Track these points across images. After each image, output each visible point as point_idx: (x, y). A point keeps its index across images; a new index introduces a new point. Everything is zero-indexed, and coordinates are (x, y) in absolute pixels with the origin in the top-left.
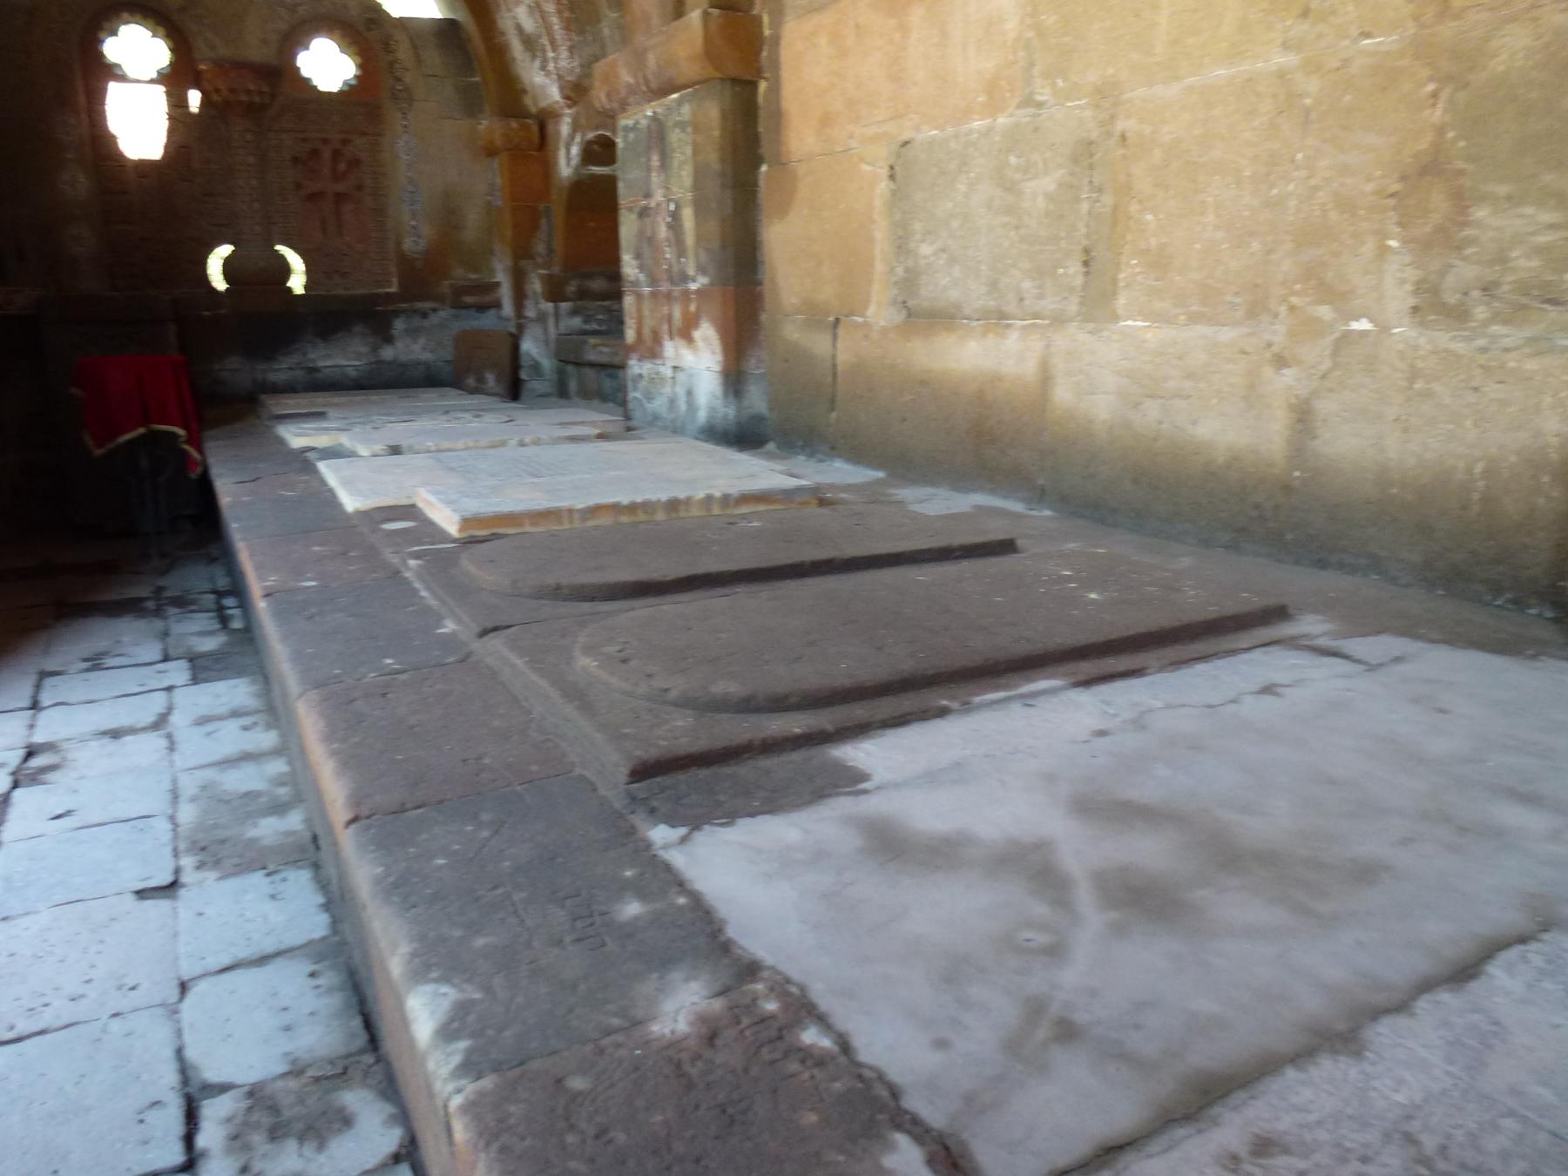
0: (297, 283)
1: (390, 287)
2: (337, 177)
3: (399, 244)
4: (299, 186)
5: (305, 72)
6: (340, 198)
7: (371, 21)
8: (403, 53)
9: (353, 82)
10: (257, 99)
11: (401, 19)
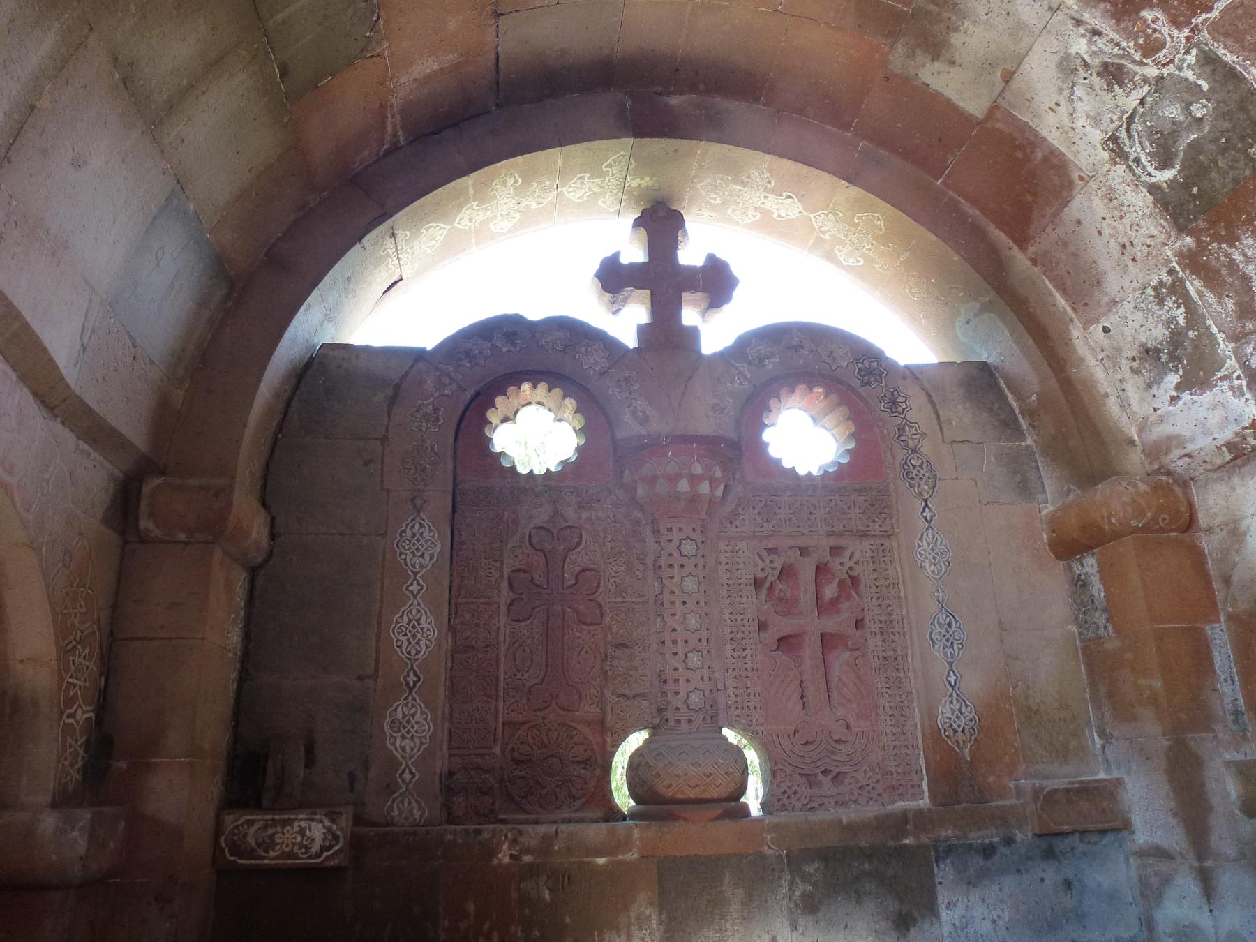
0: (753, 798)
1: (914, 797)
2: (824, 608)
3: (931, 714)
4: (762, 626)
5: (774, 452)
6: (828, 641)
7: (869, 372)
8: (917, 411)
9: (845, 460)
10: (704, 488)
11: (907, 367)
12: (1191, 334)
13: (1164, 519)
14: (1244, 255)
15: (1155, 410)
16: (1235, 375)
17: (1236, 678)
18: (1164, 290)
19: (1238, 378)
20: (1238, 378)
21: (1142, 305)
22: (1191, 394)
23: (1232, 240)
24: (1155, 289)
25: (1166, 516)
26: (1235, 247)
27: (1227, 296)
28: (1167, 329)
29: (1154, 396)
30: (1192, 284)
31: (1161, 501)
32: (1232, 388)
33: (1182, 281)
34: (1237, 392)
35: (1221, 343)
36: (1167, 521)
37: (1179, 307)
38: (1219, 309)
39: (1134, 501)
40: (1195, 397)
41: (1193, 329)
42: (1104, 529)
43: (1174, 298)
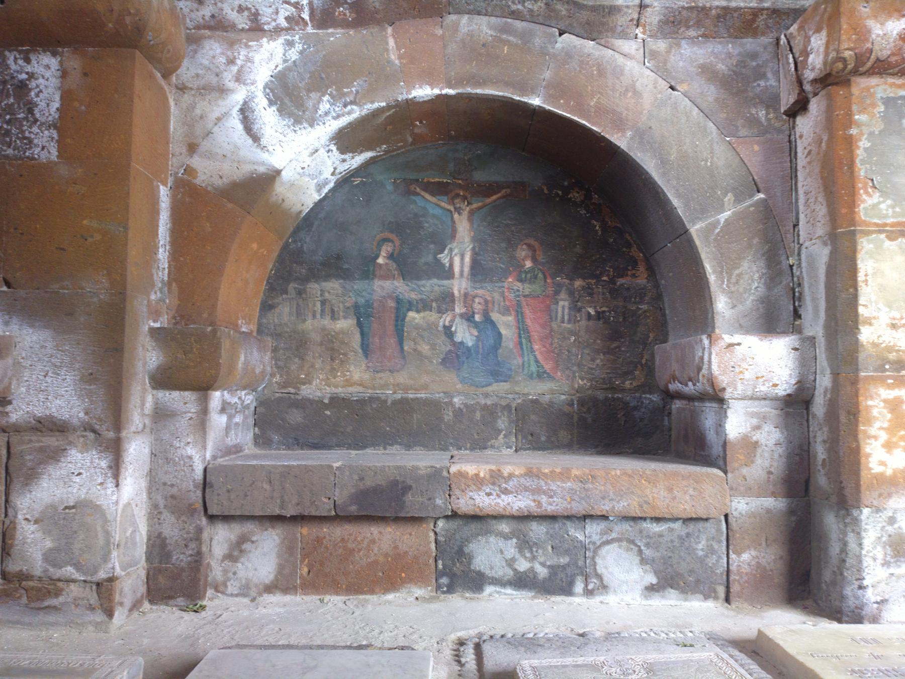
36: (168, 56)
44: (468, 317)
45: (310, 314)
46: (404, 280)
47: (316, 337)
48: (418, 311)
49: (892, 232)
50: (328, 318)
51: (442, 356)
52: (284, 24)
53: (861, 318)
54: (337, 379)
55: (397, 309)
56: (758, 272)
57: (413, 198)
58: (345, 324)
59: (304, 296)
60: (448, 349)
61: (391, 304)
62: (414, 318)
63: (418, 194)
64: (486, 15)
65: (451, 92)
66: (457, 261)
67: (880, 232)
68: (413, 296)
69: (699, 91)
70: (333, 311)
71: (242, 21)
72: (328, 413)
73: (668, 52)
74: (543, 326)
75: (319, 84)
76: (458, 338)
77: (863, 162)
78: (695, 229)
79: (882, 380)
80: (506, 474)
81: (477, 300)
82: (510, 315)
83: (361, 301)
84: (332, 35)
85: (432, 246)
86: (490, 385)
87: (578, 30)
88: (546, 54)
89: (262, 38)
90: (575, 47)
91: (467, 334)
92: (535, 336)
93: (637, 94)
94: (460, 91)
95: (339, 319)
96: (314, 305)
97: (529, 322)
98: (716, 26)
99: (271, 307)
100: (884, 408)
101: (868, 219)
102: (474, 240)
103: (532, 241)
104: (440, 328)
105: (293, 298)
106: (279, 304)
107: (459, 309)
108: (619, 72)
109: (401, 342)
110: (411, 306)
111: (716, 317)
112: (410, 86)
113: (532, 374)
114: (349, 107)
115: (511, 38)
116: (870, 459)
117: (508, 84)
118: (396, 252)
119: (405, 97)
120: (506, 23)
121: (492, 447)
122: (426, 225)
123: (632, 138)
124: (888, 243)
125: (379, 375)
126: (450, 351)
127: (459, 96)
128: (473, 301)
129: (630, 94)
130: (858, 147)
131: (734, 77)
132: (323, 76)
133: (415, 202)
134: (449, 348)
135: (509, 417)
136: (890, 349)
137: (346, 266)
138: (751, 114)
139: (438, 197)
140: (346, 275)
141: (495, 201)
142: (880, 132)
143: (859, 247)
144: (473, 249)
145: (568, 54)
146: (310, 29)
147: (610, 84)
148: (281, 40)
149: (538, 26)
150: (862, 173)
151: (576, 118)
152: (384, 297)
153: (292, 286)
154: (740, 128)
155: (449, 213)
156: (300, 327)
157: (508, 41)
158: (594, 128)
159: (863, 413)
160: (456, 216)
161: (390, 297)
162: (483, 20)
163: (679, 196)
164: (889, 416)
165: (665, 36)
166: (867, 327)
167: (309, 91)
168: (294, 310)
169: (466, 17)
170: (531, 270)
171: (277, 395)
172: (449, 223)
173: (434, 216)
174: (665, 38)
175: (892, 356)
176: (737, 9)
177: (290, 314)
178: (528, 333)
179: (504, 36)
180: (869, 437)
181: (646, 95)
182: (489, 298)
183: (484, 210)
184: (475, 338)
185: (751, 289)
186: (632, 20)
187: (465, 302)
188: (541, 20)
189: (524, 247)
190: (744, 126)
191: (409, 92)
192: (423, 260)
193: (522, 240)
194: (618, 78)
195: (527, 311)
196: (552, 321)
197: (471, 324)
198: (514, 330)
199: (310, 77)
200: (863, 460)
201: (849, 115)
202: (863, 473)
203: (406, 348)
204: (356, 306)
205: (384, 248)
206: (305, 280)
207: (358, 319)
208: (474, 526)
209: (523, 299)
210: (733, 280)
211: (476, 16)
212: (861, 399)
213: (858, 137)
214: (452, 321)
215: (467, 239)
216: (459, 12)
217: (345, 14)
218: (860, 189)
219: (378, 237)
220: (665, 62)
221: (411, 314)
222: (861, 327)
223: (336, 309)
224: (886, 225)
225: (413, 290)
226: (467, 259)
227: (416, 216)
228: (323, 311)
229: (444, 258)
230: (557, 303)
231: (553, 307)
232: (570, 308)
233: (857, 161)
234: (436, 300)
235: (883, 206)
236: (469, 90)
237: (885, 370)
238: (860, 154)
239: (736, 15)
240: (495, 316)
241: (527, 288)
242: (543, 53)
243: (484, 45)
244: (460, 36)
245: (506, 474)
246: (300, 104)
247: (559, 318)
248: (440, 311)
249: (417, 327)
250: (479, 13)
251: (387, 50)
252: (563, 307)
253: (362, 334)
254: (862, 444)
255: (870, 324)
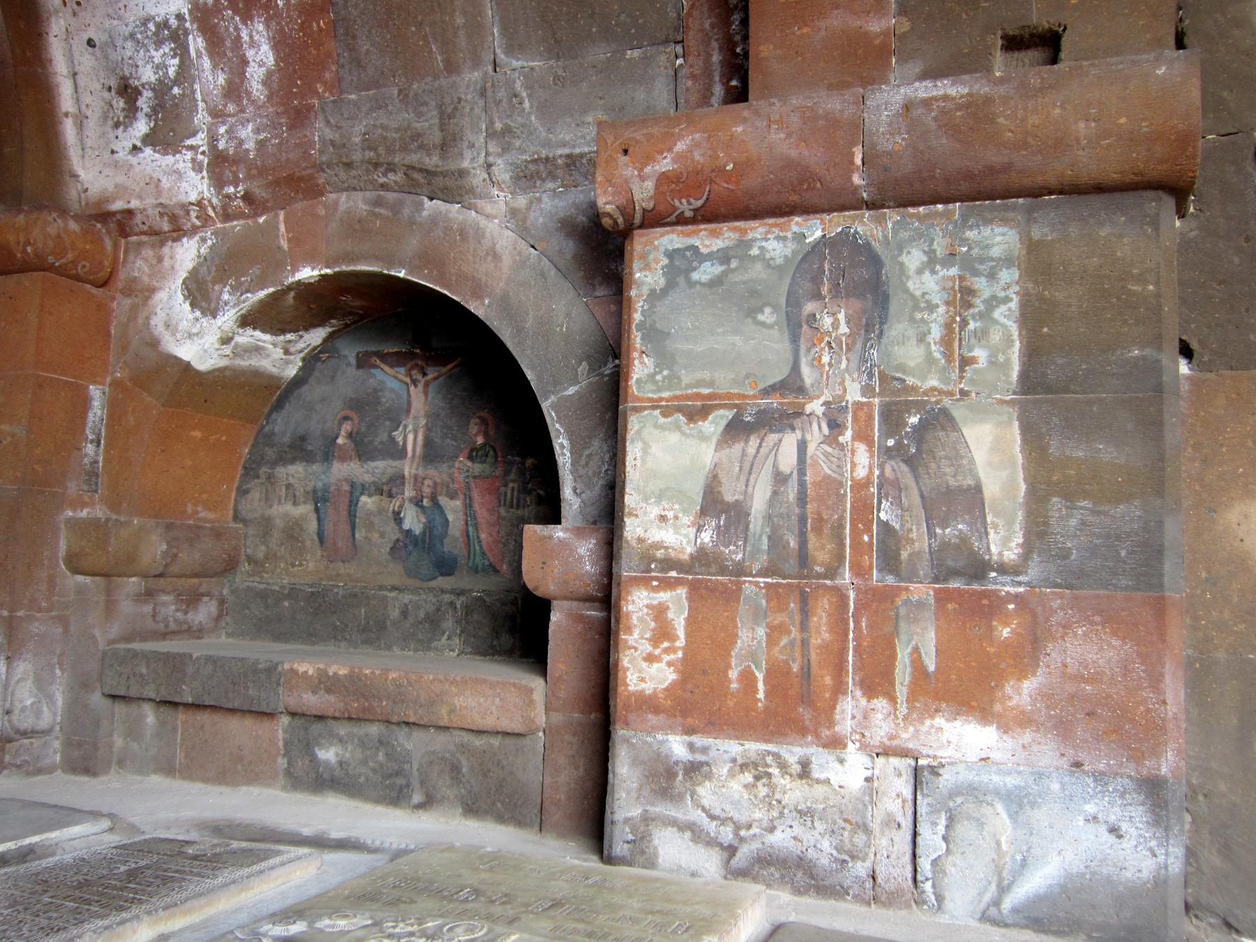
12: (176, 90)
13: (84, 266)
14: (251, 37)
15: (113, 152)
16: (201, 149)
17: (102, 442)
18: (166, 32)
19: (203, 153)
20: (203, 153)
21: (139, 36)
22: (155, 151)
23: (247, 18)
24: (158, 26)
25: (87, 264)
26: (246, 25)
27: (222, 69)
28: (155, 73)
29: (117, 137)
30: (195, 39)
31: (88, 247)
32: (193, 160)
33: (186, 33)
34: (197, 167)
35: (200, 111)
37: (174, 57)
38: (210, 78)
39: (59, 236)
40: (157, 155)
41: (179, 86)
42: (15, 256)
43: (173, 45)
44: (418, 502)
45: (276, 500)
46: (360, 460)
47: (279, 523)
48: (370, 496)
49: (667, 406)
50: (291, 503)
51: (391, 545)
52: (198, 223)
53: (627, 510)
54: (295, 569)
55: (351, 493)
56: (609, 452)
57: (373, 371)
58: (304, 510)
59: (273, 480)
60: (396, 537)
61: (346, 487)
62: (366, 503)
63: (379, 367)
64: (361, 190)
65: (329, 271)
66: (411, 437)
67: (654, 408)
68: (367, 478)
69: (557, 248)
70: (295, 496)
71: (166, 226)
72: (286, 604)
73: (529, 208)
74: (490, 511)
75: (221, 279)
76: (406, 526)
77: (641, 326)
78: (547, 406)
79: (645, 582)
80: (331, 674)
81: (426, 482)
82: (459, 499)
83: (320, 485)
84: (235, 226)
85: (388, 423)
86: (434, 578)
87: (441, 196)
88: (414, 223)
89: (184, 236)
90: (440, 213)
91: (416, 520)
92: (481, 521)
93: (496, 257)
94: (337, 269)
95: (299, 504)
96: (280, 490)
97: (476, 506)
98: (571, 175)
99: (246, 492)
100: (647, 614)
101: (640, 395)
102: (427, 416)
103: (484, 414)
104: (390, 514)
105: (263, 483)
106: (251, 489)
107: (409, 492)
108: (479, 234)
109: (353, 528)
110: (364, 489)
111: (563, 505)
112: (295, 269)
113: (477, 568)
114: (244, 297)
115: (383, 211)
116: (628, 674)
117: (377, 259)
118: (355, 430)
119: (291, 280)
120: (379, 196)
121: (436, 649)
122: (384, 400)
123: (489, 306)
124: (662, 420)
125: (332, 565)
126: (398, 540)
127: (336, 275)
128: (423, 483)
129: (490, 258)
130: (636, 311)
131: (595, 229)
132: (226, 268)
133: (374, 376)
134: (398, 535)
135: (453, 616)
136: (658, 546)
137: (310, 448)
138: (610, 270)
139: (396, 369)
140: (308, 457)
141: (450, 370)
142: (661, 290)
143: (629, 427)
144: (427, 424)
145: (434, 221)
146: (219, 225)
147: (471, 249)
148: (197, 238)
149: (407, 196)
150: (638, 340)
151: (438, 288)
152: (339, 481)
153: (264, 470)
154: (597, 287)
155: (406, 387)
156: (268, 512)
157: (380, 214)
158: (454, 297)
159: (623, 621)
160: (412, 388)
161: (346, 480)
162: (358, 196)
163: (533, 368)
164: (653, 624)
165: (524, 191)
166: (633, 518)
167: (215, 282)
168: (263, 495)
169: (345, 194)
170: (484, 445)
171: (246, 584)
172: (405, 396)
173: (392, 390)
174: (525, 193)
175: (660, 554)
176: (582, 155)
177: (260, 500)
178: (475, 519)
179: (377, 210)
180: (630, 648)
181: (504, 257)
182: (438, 480)
183: (441, 379)
184: (421, 525)
185: (600, 472)
186: (484, 180)
187: (415, 484)
188: (406, 189)
189: (478, 420)
190: (601, 284)
191: (293, 275)
192: (378, 440)
193: (474, 414)
194: (479, 242)
195: (476, 494)
196: (500, 505)
197: (419, 510)
198: (461, 516)
199: (216, 271)
200: (620, 674)
201: (631, 274)
202: (621, 689)
203: (357, 536)
204: (315, 491)
205: (344, 426)
206: (274, 464)
207: (316, 505)
208: (317, 727)
209: (472, 480)
210: (583, 462)
211: (354, 193)
212: (623, 603)
213: (637, 299)
214: (401, 506)
215: (422, 413)
216: (341, 190)
217: (240, 207)
218: (634, 359)
219: (343, 413)
220: (524, 221)
221: (364, 499)
222: (626, 519)
223: (297, 494)
224: (661, 399)
225: (368, 472)
226: (420, 437)
227: (376, 391)
228: (286, 495)
229: (398, 436)
230: (506, 485)
231: (503, 489)
232: (519, 491)
233: (634, 327)
234: (387, 483)
235: (659, 377)
236: (344, 268)
237: (650, 571)
238: (637, 316)
239: (584, 161)
240: (443, 500)
241: (477, 468)
242: (412, 222)
243: (359, 221)
244: (339, 215)
245: (331, 674)
246: (206, 297)
247: (508, 503)
248: (390, 496)
249: (369, 514)
250: (355, 189)
251: (278, 237)
252: (513, 488)
253: (319, 520)
254: (621, 655)
255: (636, 516)
